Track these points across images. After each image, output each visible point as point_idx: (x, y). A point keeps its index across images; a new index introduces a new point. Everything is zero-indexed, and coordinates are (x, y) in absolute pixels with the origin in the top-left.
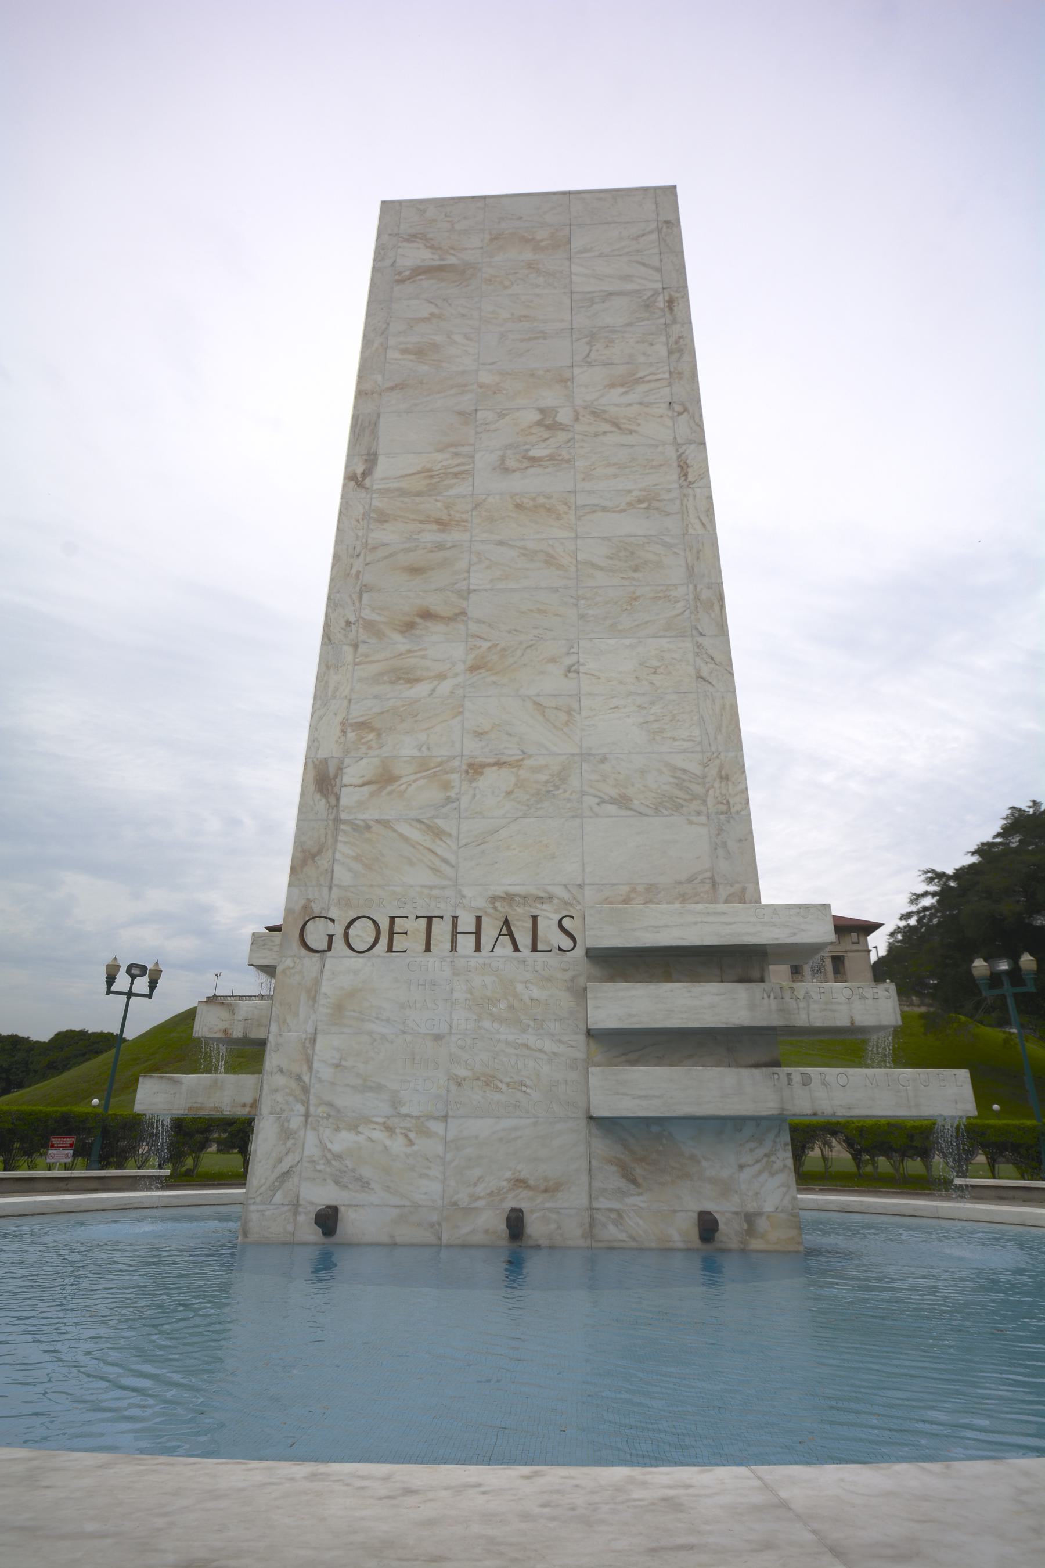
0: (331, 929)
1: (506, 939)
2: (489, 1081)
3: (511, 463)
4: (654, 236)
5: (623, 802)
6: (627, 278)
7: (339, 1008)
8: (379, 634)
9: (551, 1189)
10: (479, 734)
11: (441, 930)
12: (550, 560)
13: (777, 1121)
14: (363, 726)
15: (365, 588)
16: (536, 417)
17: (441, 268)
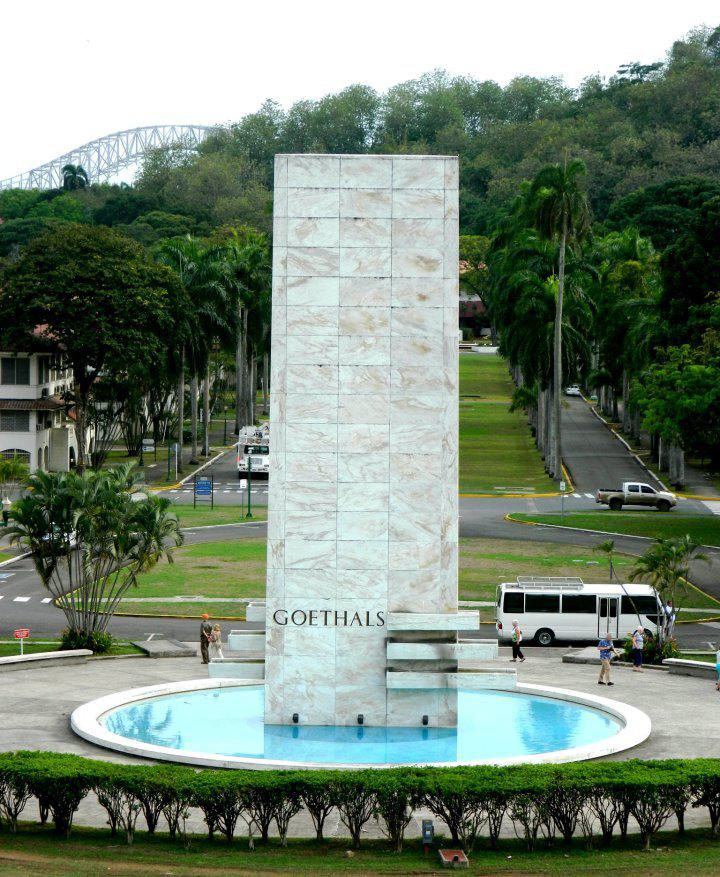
0: (286, 615)
1: (357, 621)
11: (331, 619)
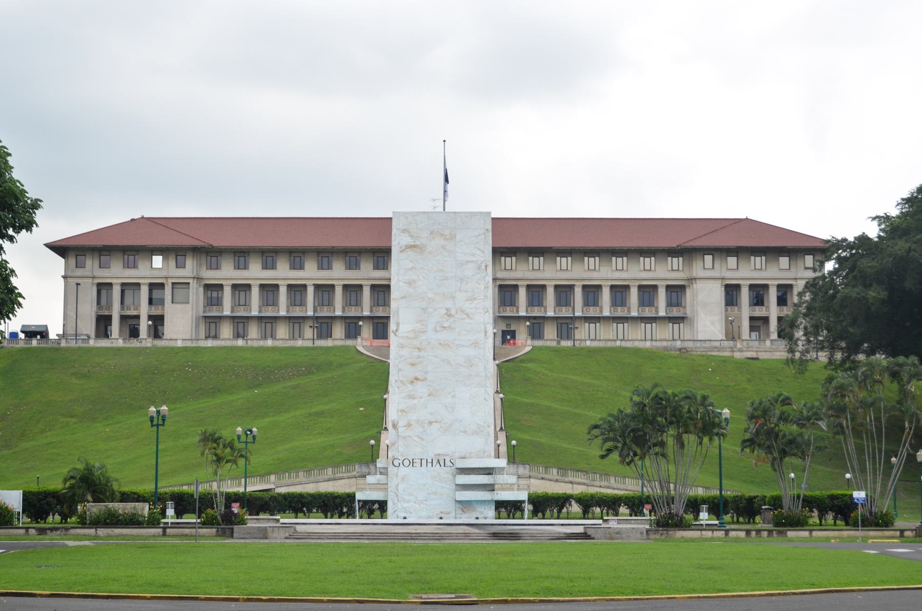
2: (435, 493)
3: (438, 329)
4: (482, 236)
5: (465, 432)
6: (473, 255)
7: (403, 479)
8: (404, 384)
9: (448, 513)
10: (431, 414)
11: (424, 462)
12: (449, 363)
13: (492, 501)
14: (402, 411)
15: (400, 370)
16: (445, 311)
17: (414, 246)
